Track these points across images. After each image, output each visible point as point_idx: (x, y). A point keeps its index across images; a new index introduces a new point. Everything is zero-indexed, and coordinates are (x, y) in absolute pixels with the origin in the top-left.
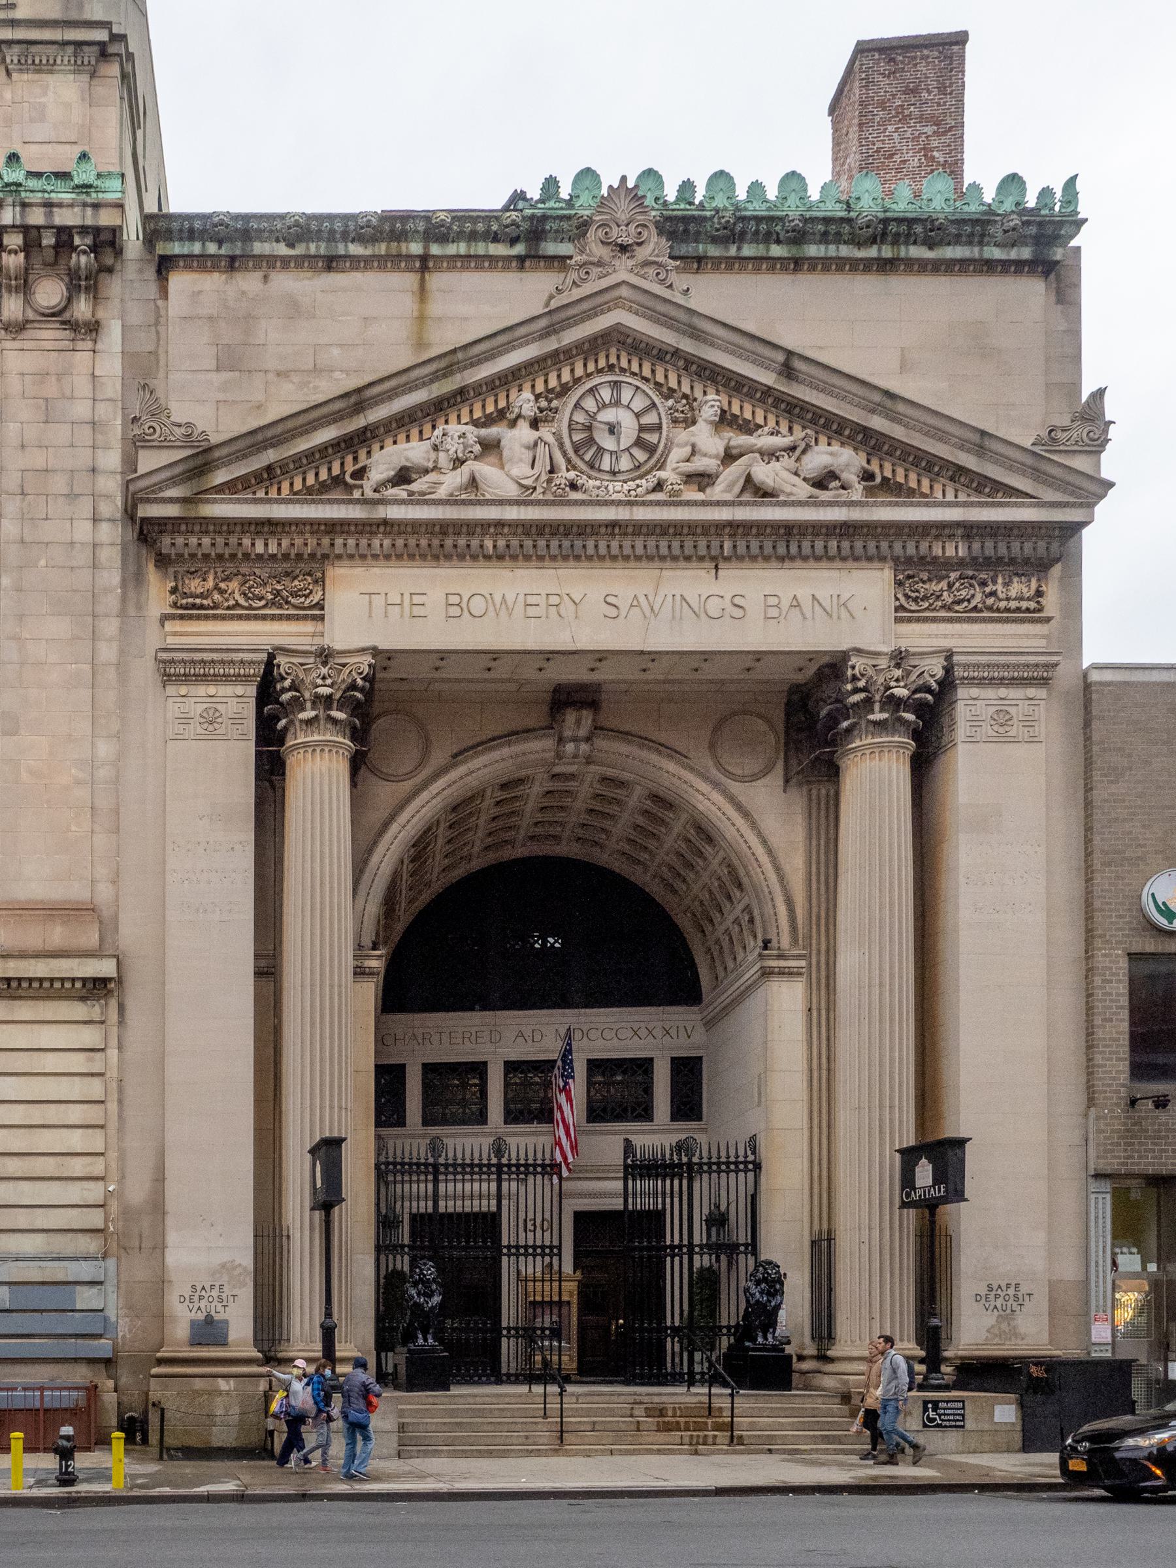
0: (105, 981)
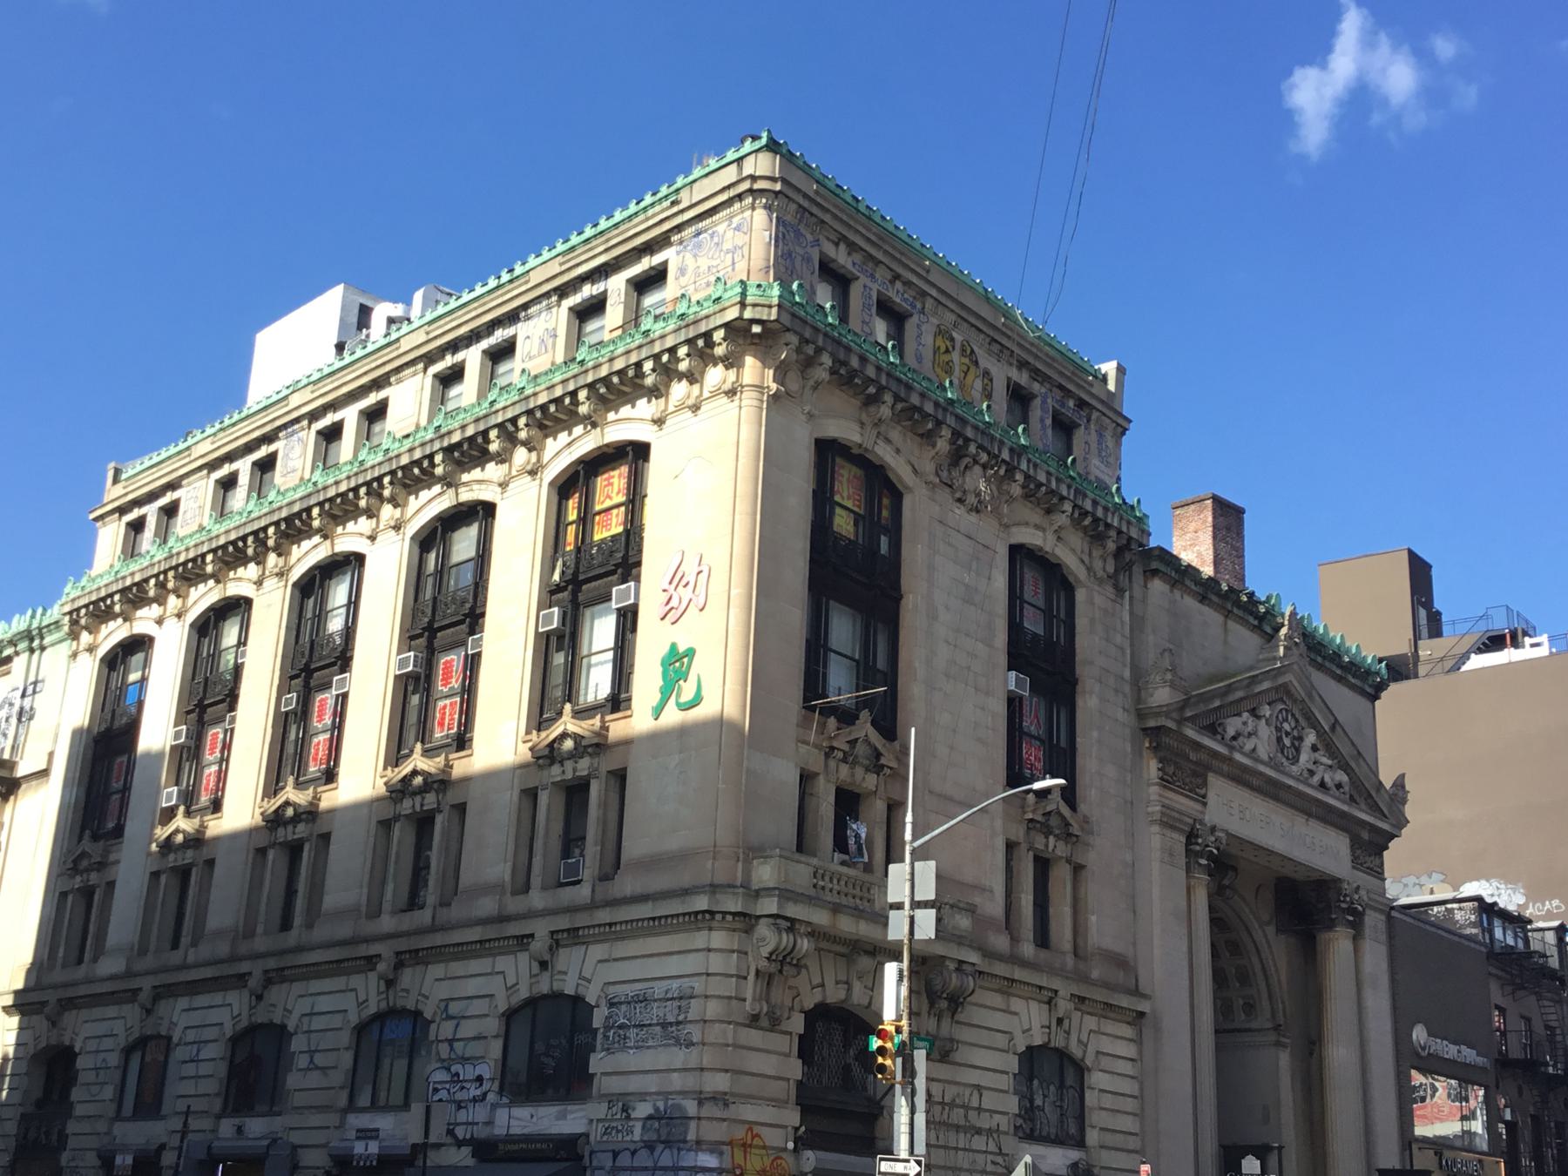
0: (1142, 1014)
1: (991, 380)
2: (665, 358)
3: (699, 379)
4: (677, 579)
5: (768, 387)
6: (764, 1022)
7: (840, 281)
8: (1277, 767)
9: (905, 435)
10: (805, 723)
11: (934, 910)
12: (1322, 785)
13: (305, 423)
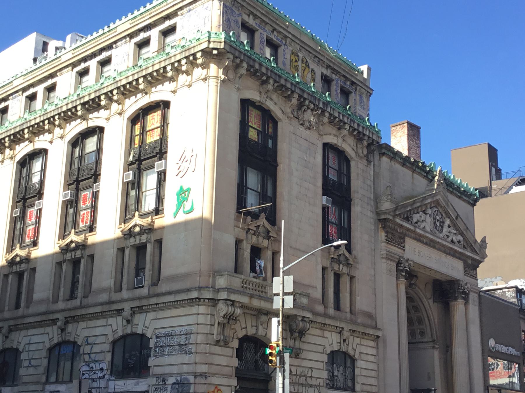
0: (378, 337)
1: (315, 74)
2: (176, 65)
3: (191, 73)
4: (182, 158)
5: (220, 77)
6: (222, 343)
7: (251, 32)
8: (434, 234)
9: (278, 97)
10: (237, 219)
11: (292, 296)
12: (452, 241)
13: (20, 93)
